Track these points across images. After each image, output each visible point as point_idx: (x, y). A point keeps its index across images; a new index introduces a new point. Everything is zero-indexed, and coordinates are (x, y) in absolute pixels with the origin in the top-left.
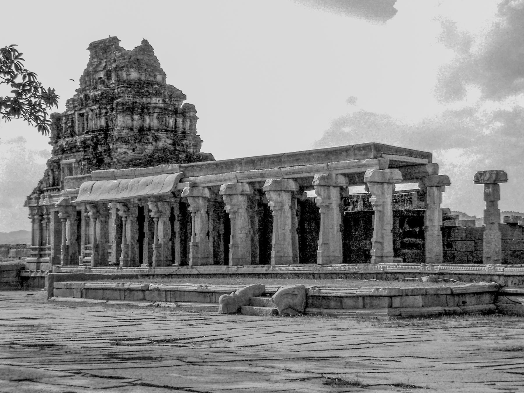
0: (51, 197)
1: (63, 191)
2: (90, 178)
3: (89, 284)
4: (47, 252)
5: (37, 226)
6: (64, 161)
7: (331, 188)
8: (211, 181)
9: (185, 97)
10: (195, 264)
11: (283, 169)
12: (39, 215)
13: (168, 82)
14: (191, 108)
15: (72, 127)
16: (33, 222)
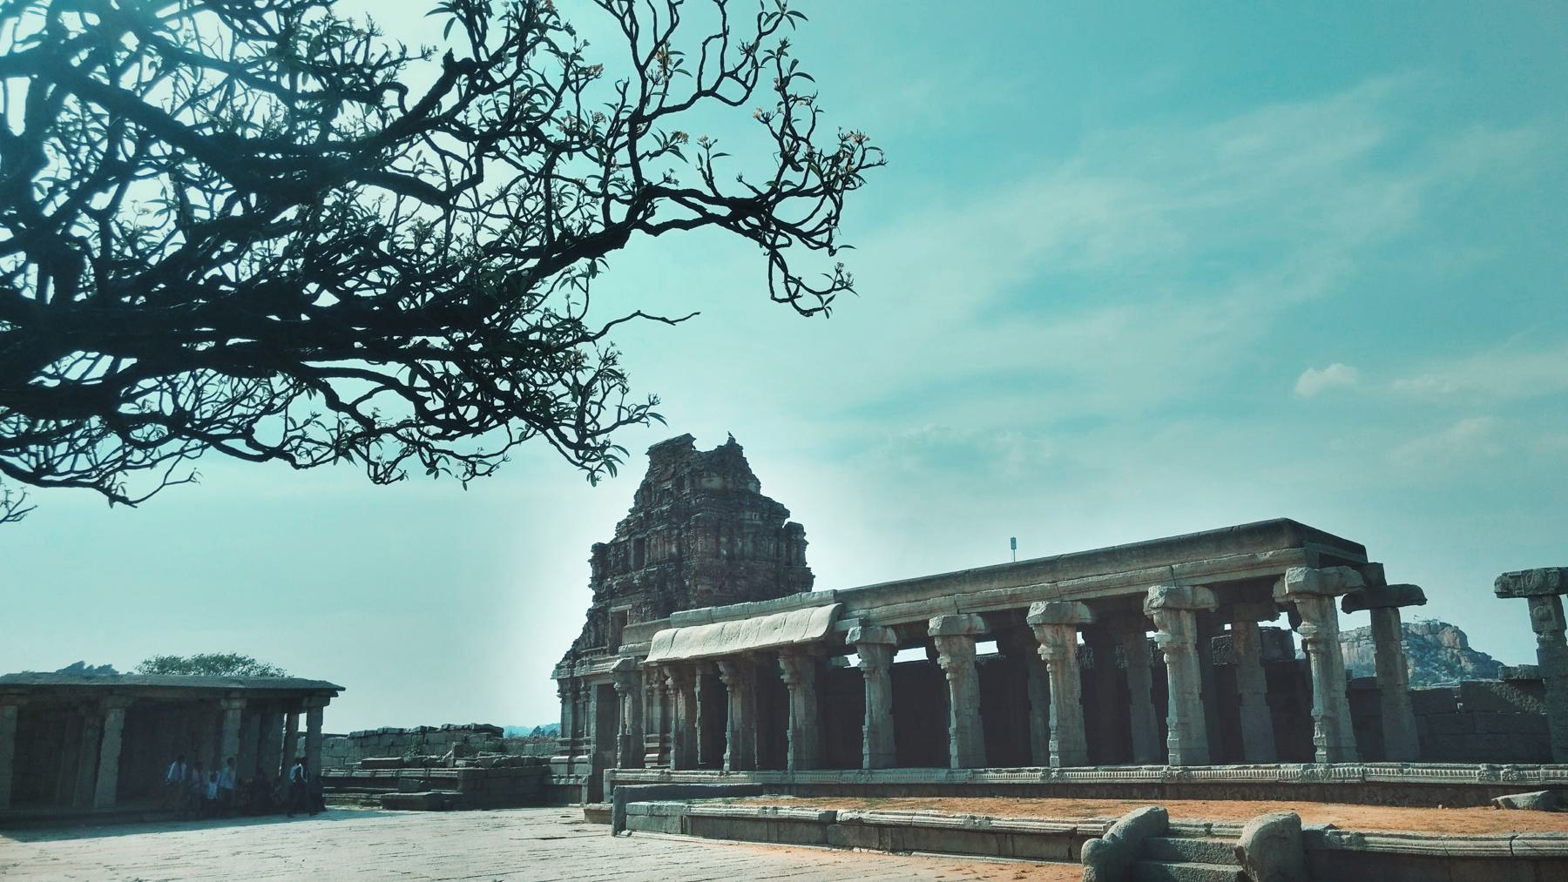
0: (592, 663)
1: (621, 649)
2: (668, 626)
3: (701, 808)
4: (585, 747)
5: (569, 709)
6: (613, 609)
7: (1183, 613)
8: (901, 615)
9: (787, 514)
10: (873, 767)
11: (1061, 584)
12: (571, 688)
13: (764, 492)
14: (797, 529)
15: (626, 558)
16: (563, 702)
